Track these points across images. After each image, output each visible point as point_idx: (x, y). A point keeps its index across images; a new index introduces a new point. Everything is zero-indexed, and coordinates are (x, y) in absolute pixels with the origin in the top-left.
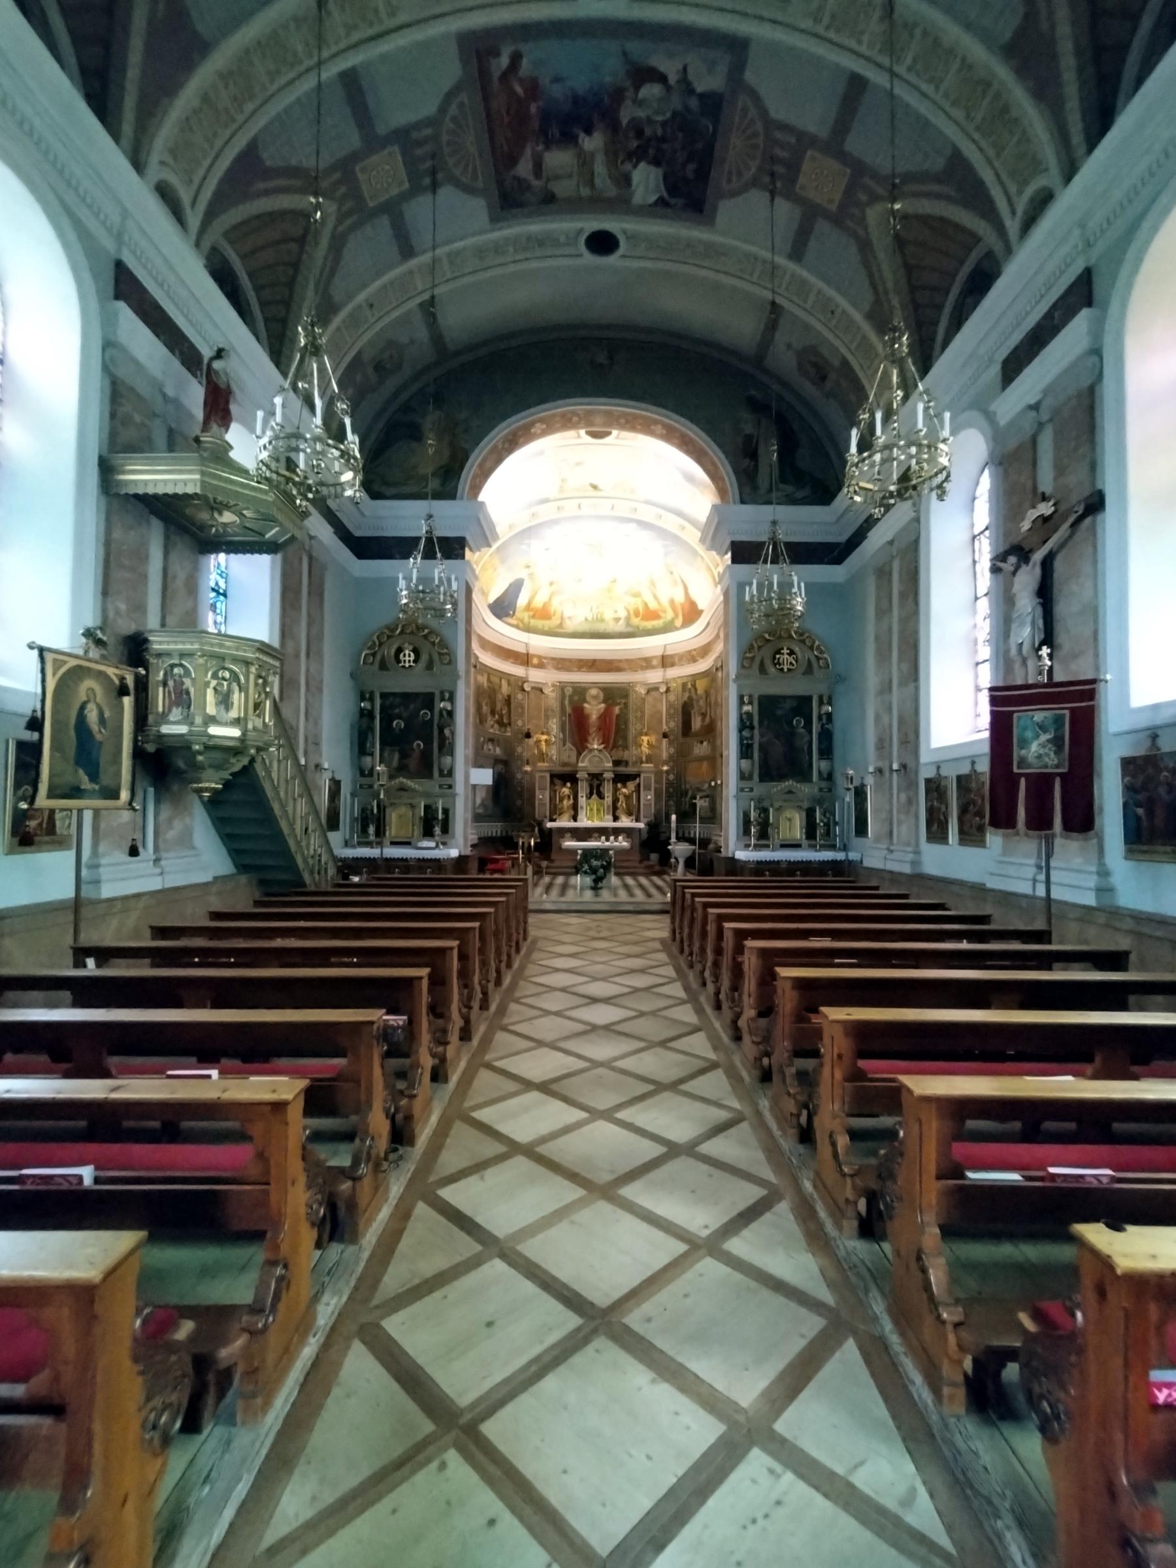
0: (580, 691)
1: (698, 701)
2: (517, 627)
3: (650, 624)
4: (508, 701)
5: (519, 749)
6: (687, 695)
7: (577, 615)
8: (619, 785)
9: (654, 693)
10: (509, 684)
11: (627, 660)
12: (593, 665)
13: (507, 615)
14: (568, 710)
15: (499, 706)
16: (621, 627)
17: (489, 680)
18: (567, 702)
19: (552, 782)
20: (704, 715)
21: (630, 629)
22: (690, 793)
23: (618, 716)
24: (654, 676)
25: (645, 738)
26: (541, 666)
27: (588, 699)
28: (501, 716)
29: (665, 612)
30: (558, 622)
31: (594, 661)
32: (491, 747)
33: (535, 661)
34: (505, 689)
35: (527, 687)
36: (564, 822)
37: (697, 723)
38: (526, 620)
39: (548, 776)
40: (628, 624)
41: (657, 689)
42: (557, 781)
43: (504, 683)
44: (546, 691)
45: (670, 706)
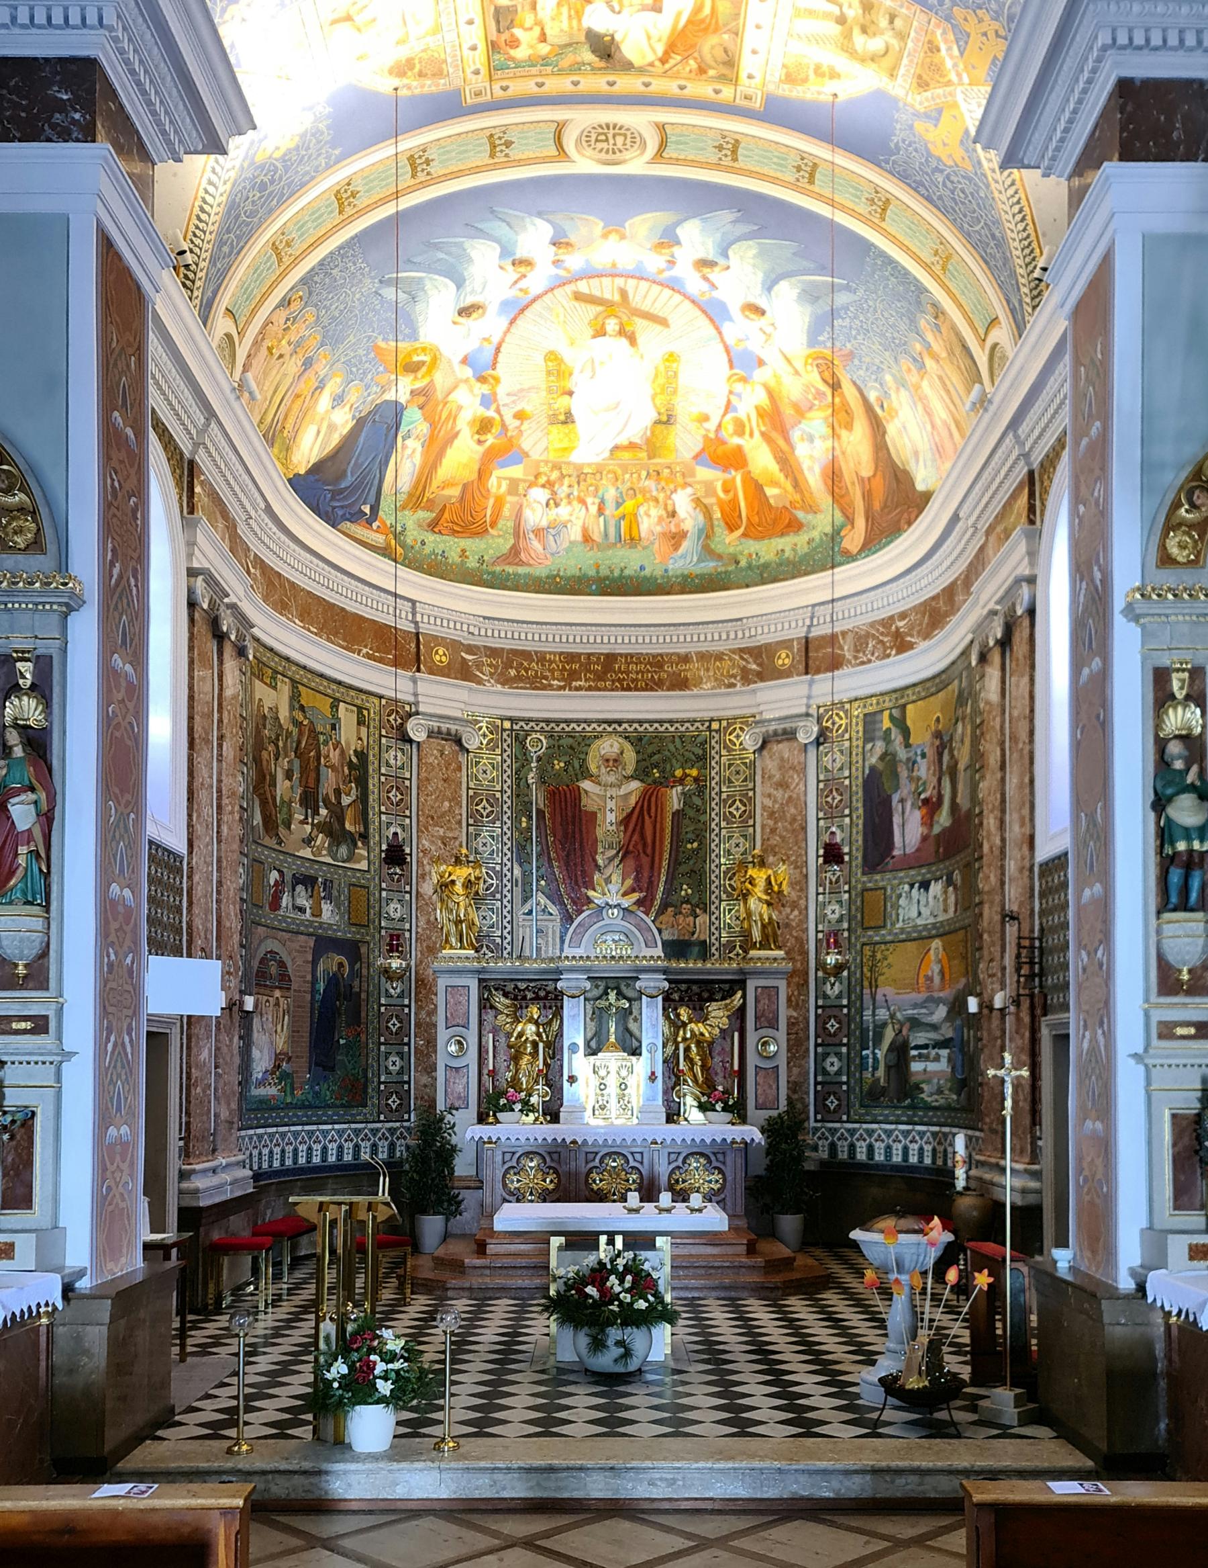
0: (570, 744)
1: (912, 764)
2: (385, 552)
3: (767, 550)
4: (359, 769)
5: (394, 909)
6: (880, 747)
7: (561, 524)
8: (684, 1013)
9: (782, 749)
10: (360, 723)
11: (703, 656)
12: (607, 670)
13: (356, 516)
14: (538, 797)
16: (685, 560)
17: (295, 697)
18: (532, 778)
19: (485, 1004)
20: (931, 806)
21: (709, 566)
23: (676, 814)
24: (782, 699)
26: (464, 672)
27: (593, 768)
28: (338, 813)
29: (813, 509)
30: (506, 544)
31: (611, 658)
33: (441, 656)
34: (349, 734)
37: (909, 830)
38: (413, 535)
40: (708, 551)
41: (789, 735)
42: (500, 1001)
43: (346, 715)
44: (473, 742)
45: (829, 785)
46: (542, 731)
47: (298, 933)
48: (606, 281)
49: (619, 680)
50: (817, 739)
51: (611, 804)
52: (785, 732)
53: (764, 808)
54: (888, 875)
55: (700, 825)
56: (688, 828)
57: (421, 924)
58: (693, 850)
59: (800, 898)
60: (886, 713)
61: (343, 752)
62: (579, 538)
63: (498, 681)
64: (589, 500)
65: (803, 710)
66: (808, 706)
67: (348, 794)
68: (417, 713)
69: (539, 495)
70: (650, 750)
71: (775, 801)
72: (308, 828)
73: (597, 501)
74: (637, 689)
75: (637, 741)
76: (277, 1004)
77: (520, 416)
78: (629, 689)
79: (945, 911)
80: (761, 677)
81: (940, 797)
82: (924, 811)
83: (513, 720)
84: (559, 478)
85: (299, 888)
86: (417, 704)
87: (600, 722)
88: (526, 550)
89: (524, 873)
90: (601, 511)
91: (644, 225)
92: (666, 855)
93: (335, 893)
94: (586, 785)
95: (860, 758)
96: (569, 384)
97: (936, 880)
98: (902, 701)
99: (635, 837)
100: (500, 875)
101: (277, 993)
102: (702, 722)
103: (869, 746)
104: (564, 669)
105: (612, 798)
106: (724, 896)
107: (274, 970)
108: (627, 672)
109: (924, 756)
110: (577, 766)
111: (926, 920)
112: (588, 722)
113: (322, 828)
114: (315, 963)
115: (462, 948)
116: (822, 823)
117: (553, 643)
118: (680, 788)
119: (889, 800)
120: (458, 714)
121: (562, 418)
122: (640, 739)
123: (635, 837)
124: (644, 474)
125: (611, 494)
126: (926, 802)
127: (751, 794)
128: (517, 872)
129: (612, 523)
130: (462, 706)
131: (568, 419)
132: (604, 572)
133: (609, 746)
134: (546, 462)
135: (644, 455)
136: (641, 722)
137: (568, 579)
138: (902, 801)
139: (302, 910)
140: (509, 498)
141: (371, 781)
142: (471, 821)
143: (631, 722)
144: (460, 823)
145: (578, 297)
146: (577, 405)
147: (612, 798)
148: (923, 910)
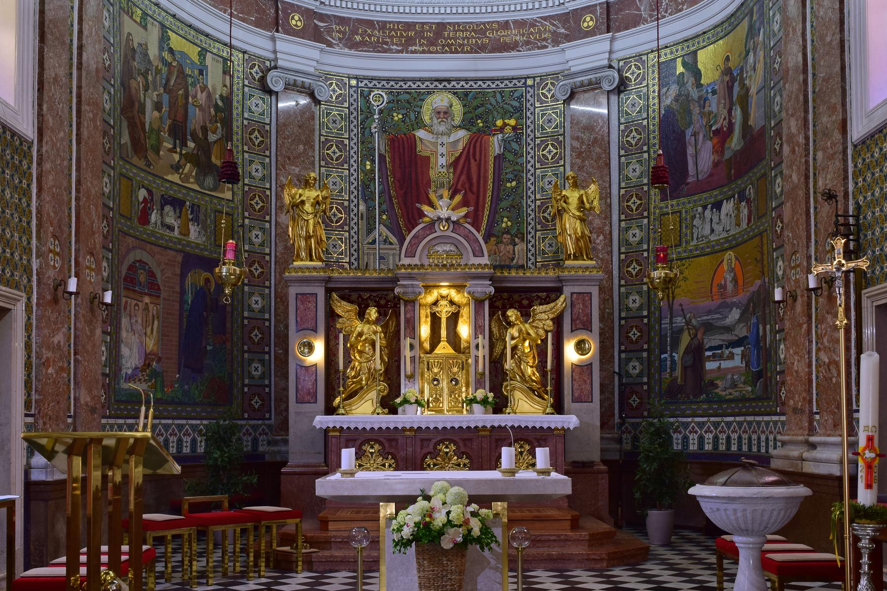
0: (408, 97)
1: (703, 101)
6: (674, 90)
14: (379, 143)
15: (196, 118)
17: (164, 39)
18: (374, 127)
20: (722, 136)
22: (685, 339)
23: (497, 158)
25: (573, 196)
27: (426, 118)
28: (205, 147)
31: (442, 26)
32: (170, 220)
33: (296, 21)
35: (275, 81)
36: (364, 412)
37: (702, 158)
39: (321, 292)
42: (343, 308)
47: (165, 248)
49: (449, 45)
50: (618, 87)
51: (441, 150)
52: (590, 83)
53: (573, 149)
54: (682, 200)
55: (518, 167)
56: (508, 169)
57: (280, 248)
58: (512, 188)
59: (604, 225)
60: (679, 61)
61: (209, 96)
63: (346, 46)
65: (606, 62)
66: (609, 59)
67: (214, 132)
68: (276, 67)
70: (475, 103)
71: (582, 143)
72: (176, 157)
74: (463, 52)
75: (463, 96)
76: (146, 309)
78: (457, 52)
79: (738, 225)
80: (568, 38)
81: (731, 125)
82: (715, 140)
85: (168, 208)
86: (276, 59)
92: (489, 193)
93: (202, 217)
94: (421, 134)
95: (656, 101)
97: (728, 199)
98: (692, 49)
99: (463, 178)
100: (348, 210)
101: (147, 300)
102: (519, 79)
103: (665, 90)
105: (442, 144)
106: (539, 227)
107: (142, 277)
108: (455, 39)
109: (714, 92)
110: (413, 118)
111: (720, 235)
112: (422, 80)
113: (188, 157)
114: (183, 276)
115: (311, 260)
116: (623, 159)
118: (500, 136)
119: (683, 133)
120: (311, 70)
122: (466, 95)
123: (463, 178)
126: (717, 132)
127: (561, 138)
128: (362, 207)
130: (315, 64)
133: (440, 100)
136: (467, 80)
138: (695, 134)
139: (171, 228)
141: (235, 124)
142: (323, 163)
143: (458, 80)
144: (313, 163)
147: (442, 144)
148: (715, 226)
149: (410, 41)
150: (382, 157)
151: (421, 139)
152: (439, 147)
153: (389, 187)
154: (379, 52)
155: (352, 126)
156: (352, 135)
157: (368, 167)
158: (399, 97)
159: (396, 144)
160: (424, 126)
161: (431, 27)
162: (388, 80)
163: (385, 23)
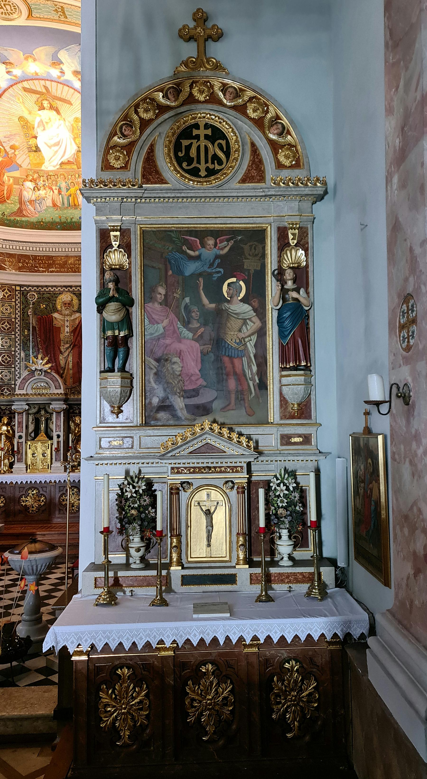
14: (33, 321)
18: (30, 312)
27: (59, 307)
46: (35, 291)
48: (36, 82)
51: (67, 324)
62: (51, 205)
64: (54, 188)
69: (30, 185)
73: (57, 188)
77: (12, 147)
83: (21, 286)
84: (37, 176)
87: (61, 287)
88: (25, 210)
89: (26, 356)
90: (60, 192)
91: (42, 52)
94: (56, 315)
96: (34, 133)
104: (45, 263)
105: (67, 321)
110: (51, 306)
112: (56, 286)
117: (29, 251)
121: (34, 149)
124: (77, 176)
125: (63, 185)
128: (23, 354)
129: (65, 198)
131: (37, 150)
132: (63, 220)
134: (31, 170)
135: (75, 167)
137: (47, 223)
140: (15, 186)
145: (26, 90)
146: (40, 143)
147: (67, 321)
149: (50, 266)
150: (34, 328)
151: (56, 318)
152: (66, 322)
153: (38, 344)
154: (33, 272)
155: (17, 311)
156: (17, 316)
157: (26, 333)
158: (45, 296)
159: (42, 321)
160: (57, 311)
161: (61, 259)
162: (38, 286)
163: (36, 256)
